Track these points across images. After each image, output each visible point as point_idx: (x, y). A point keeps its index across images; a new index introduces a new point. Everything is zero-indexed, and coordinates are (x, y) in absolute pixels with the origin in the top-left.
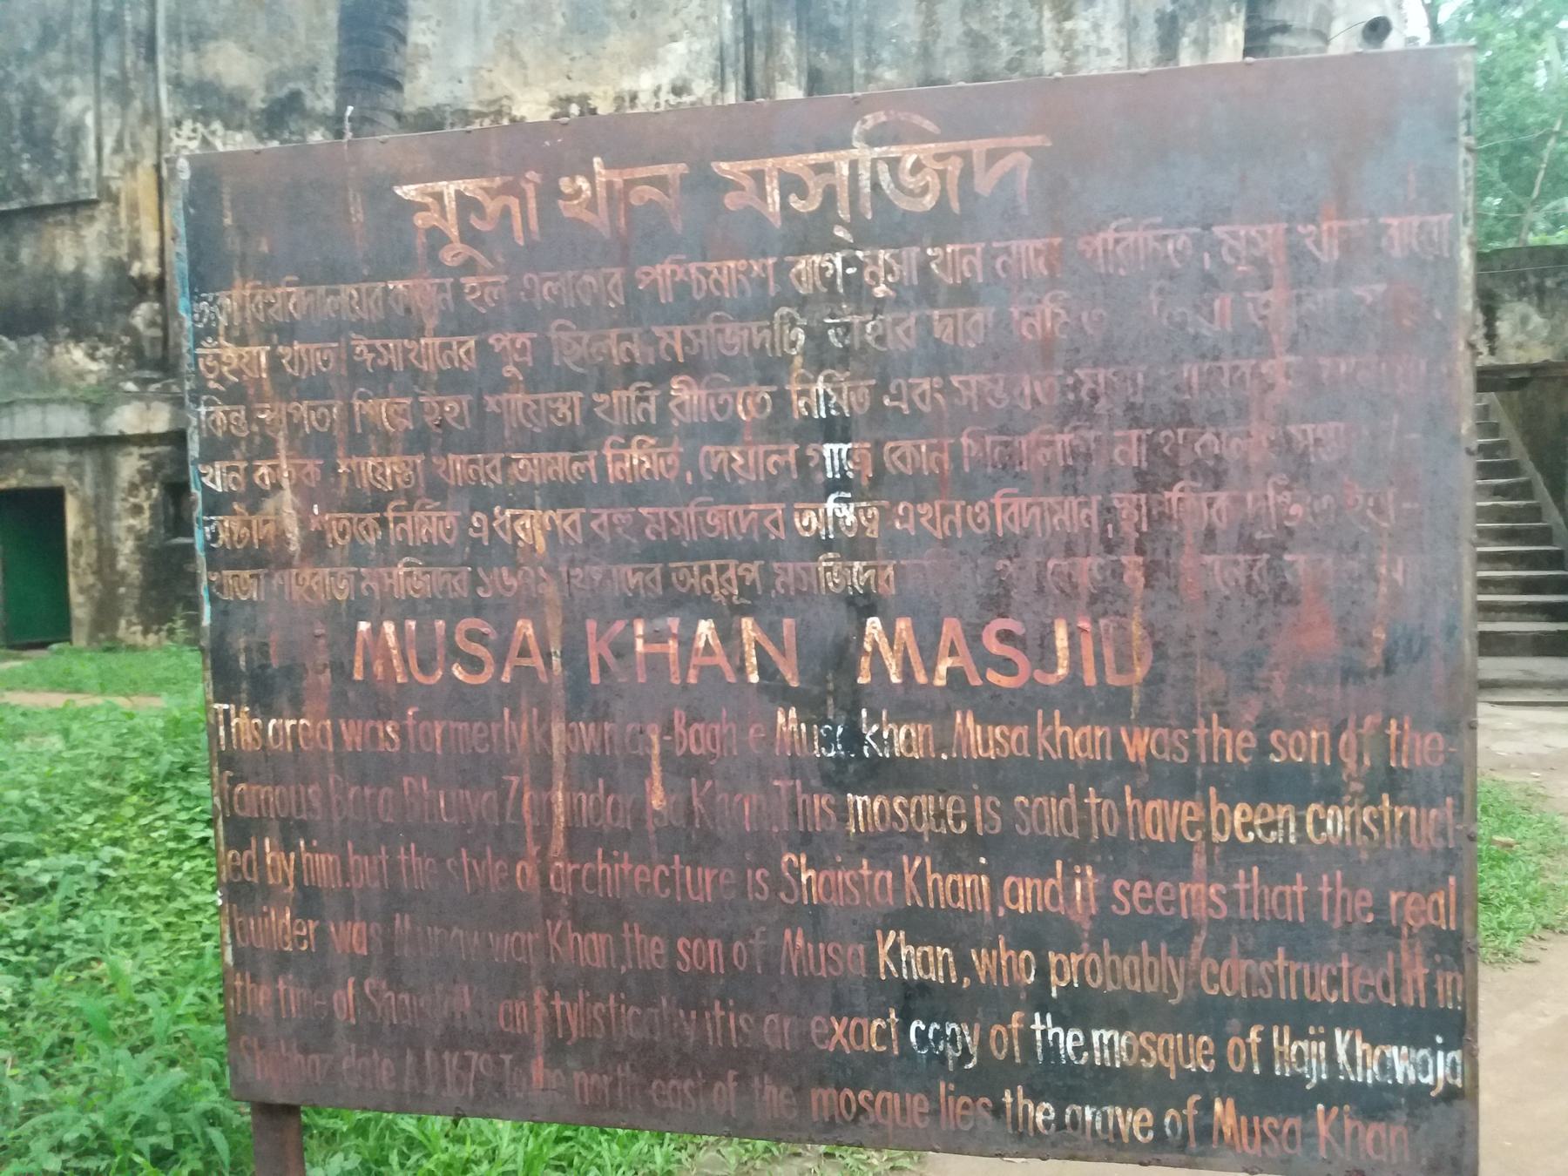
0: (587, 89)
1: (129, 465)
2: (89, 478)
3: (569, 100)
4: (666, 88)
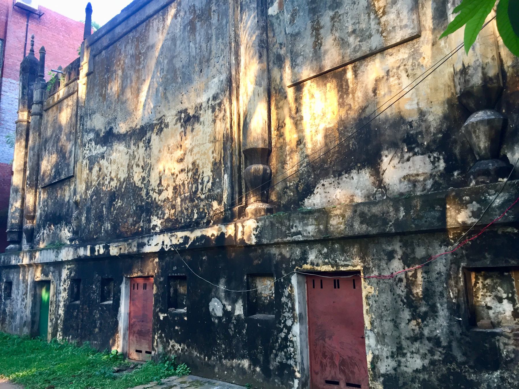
1: (65, 273)
3: (180, 112)
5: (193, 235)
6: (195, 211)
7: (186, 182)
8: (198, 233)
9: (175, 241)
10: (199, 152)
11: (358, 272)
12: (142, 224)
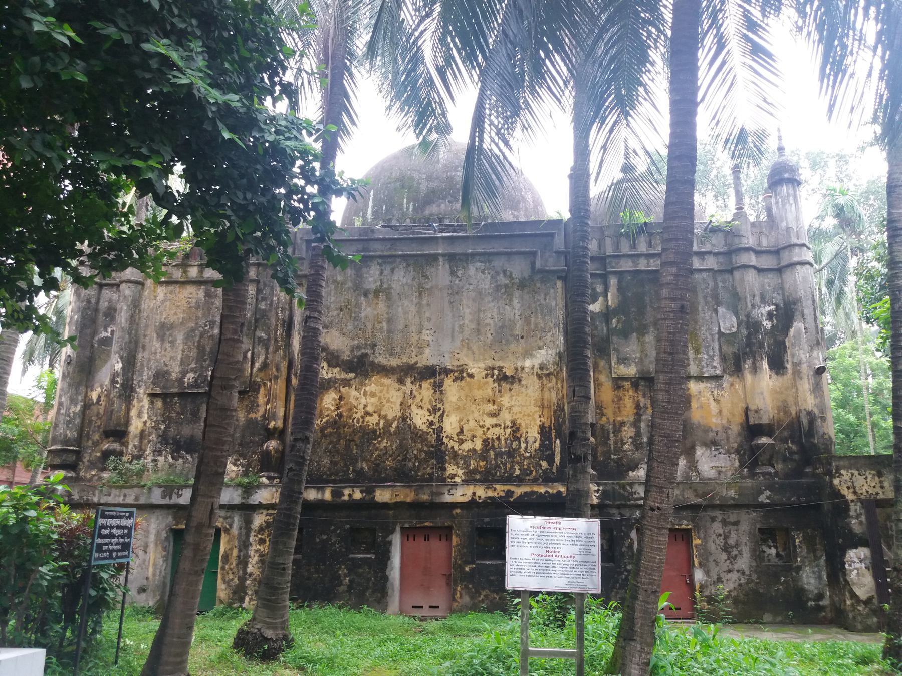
0: (500, 363)
1: (259, 520)
2: (236, 526)
3: (493, 368)
4: (537, 366)
5: (519, 491)
6: (517, 467)
7: (503, 438)
8: (527, 489)
9: (490, 494)
10: (520, 412)
11: (690, 529)
12: (429, 470)
